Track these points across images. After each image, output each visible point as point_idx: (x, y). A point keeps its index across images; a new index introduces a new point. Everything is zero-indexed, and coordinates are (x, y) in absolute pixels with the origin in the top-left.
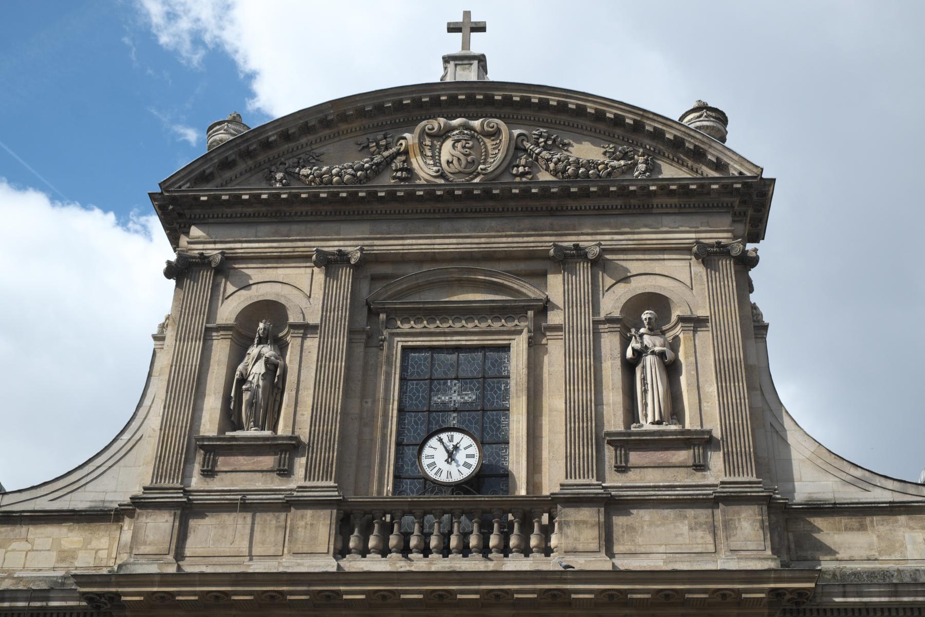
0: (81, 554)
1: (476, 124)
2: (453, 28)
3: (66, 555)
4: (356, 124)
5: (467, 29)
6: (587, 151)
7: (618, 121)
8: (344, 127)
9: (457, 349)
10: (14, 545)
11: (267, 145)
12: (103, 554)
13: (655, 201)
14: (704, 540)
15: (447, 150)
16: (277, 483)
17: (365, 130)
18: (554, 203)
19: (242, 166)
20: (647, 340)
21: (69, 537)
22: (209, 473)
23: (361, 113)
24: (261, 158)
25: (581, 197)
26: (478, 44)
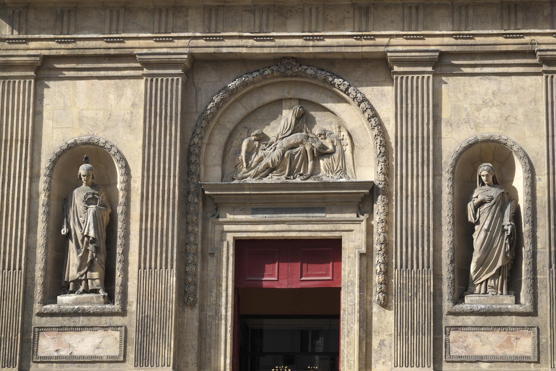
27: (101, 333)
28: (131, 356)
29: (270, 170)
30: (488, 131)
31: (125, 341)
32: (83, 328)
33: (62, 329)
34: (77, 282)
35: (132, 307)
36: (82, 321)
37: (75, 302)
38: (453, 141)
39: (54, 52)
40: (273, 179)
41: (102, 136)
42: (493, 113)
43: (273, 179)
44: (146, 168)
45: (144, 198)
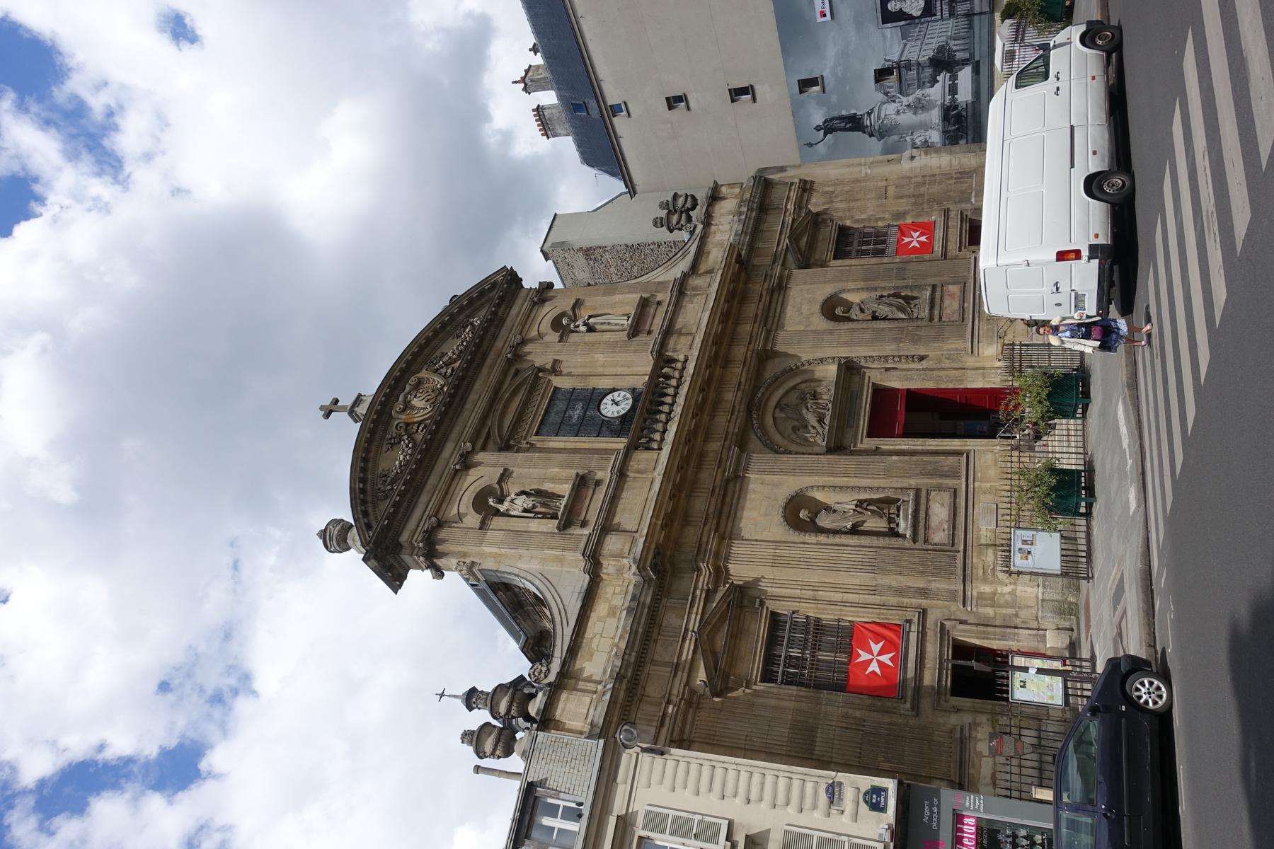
0: (614, 603)
1: (407, 389)
2: (327, 416)
3: (612, 612)
4: (374, 448)
5: (334, 407)
6: (451, 347)
7: (444, 325)
8: (371, 455)
9: (547, 412)
10: (594, 646)
11: (363, 491)
12: (618, 590)
13: (500, 314)
14: (699, 300)
15: (416, 402)
16: (603, 488)
17: (380, 446)
18: (479, 356)
19: (370, 510)
20: (580, 322)
21: (600, 609)
22: (584, 524)
23: (370, 441)
24: (369, 499)
25: (476, 356)
26: (346, 401)
27: (931, 503)
28: (950, 482)
29: (821, 421)
30: (817, 308)
31: (939, 488)
32: (927, 514)
33: (927, 527)
34: (890, 520)
35: (913, 482)
36: (922, 514)
37: (906, 519)
38: (820, 323)
39: (714, 527)
40: (827, 421)
41: (782, 500)
42: (805, 309)
43: (827, 421)
44: (811, 473)
45: (832, 474)
